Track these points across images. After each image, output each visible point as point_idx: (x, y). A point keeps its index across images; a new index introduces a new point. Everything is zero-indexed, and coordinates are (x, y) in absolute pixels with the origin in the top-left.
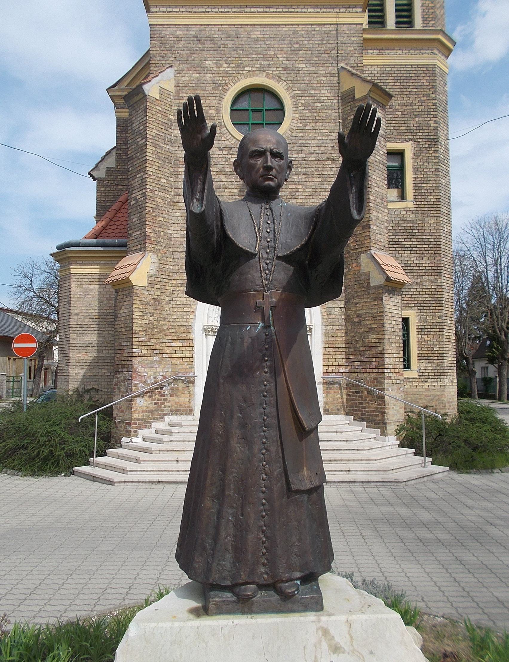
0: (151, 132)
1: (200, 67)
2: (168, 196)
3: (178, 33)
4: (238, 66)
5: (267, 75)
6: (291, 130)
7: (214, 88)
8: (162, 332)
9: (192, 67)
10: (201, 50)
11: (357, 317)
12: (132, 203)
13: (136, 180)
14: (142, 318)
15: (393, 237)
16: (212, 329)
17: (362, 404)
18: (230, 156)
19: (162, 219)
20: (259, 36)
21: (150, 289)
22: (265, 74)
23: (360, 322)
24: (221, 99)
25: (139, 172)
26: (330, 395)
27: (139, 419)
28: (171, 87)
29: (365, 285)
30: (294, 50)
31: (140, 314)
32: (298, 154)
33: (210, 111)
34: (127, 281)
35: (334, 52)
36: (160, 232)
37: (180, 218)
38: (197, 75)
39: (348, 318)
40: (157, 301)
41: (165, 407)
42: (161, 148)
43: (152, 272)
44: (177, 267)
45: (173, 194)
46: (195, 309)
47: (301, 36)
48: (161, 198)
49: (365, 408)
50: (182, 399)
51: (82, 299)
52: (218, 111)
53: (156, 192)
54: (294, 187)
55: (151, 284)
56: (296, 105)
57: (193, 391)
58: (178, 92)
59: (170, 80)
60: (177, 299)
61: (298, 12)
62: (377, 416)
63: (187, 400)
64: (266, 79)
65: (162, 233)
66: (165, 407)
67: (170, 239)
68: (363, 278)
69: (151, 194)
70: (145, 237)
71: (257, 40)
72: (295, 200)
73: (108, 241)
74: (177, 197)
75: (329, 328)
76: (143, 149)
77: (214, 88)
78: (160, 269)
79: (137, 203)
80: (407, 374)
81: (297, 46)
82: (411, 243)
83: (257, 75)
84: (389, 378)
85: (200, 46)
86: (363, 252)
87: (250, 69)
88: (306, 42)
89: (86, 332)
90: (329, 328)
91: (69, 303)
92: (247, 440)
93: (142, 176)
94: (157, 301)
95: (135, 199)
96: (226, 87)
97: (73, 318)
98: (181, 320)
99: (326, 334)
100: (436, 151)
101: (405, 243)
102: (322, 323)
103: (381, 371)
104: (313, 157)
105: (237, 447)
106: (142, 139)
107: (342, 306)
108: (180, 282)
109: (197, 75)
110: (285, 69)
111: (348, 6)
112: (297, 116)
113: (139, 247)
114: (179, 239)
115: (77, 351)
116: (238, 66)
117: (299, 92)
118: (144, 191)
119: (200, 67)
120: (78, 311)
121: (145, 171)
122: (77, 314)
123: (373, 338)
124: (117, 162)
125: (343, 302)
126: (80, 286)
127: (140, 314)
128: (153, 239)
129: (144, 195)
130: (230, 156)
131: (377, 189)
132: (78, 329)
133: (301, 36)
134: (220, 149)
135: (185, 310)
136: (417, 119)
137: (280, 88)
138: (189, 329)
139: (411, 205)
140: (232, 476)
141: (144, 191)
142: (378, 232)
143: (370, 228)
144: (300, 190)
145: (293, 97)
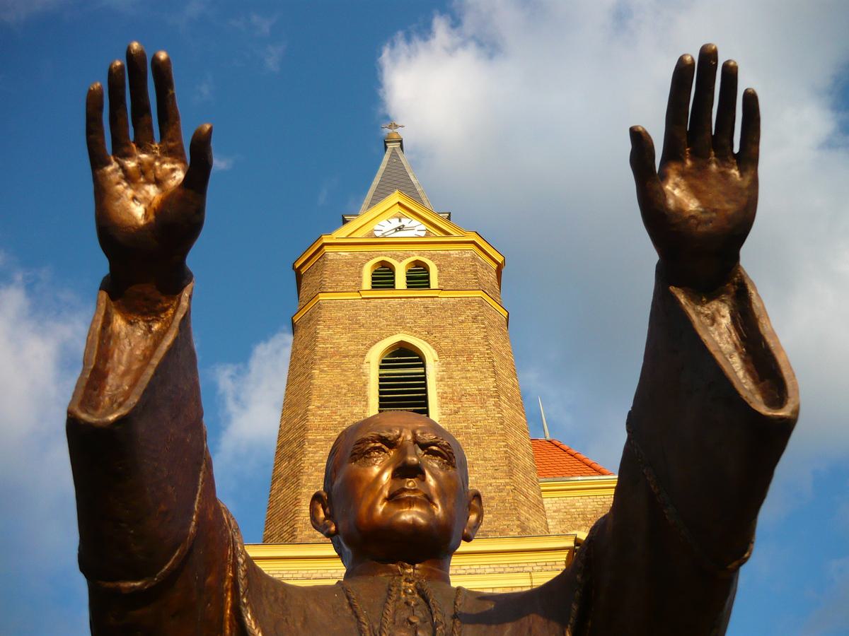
61: (470, 574)
111: (545, 564)
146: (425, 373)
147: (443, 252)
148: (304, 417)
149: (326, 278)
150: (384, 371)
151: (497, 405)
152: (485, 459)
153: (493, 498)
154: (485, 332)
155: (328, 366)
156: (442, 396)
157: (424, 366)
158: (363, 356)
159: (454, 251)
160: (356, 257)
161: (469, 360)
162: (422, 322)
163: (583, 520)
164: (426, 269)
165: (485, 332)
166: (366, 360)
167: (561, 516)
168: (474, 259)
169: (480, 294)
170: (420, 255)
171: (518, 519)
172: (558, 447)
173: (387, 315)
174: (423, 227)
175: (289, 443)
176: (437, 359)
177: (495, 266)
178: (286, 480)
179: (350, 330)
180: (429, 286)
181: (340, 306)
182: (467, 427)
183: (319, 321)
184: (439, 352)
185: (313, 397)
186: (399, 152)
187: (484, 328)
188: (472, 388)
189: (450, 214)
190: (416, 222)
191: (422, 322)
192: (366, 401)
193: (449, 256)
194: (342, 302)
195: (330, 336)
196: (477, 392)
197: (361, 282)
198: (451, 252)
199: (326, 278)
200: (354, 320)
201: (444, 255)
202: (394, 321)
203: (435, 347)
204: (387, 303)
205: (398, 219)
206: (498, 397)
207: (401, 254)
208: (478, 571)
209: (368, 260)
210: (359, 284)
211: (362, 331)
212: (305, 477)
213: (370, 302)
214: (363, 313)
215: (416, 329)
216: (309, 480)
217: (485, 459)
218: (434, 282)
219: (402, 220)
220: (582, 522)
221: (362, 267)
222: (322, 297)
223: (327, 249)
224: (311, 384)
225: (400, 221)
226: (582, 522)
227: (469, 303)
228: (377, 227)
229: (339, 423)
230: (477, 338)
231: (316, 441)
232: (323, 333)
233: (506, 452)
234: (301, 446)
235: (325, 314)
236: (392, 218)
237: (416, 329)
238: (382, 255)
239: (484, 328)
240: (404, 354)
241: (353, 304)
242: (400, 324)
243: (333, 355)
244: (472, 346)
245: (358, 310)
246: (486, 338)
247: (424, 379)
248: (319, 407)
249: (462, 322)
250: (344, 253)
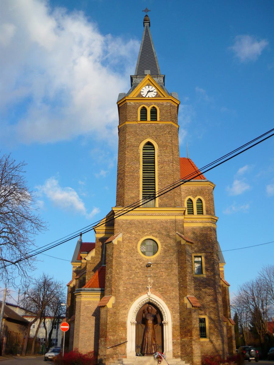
0: (115, 255)
1: (131, 233)
2: (119, 276)
3: (124, 222)
4: (143, 232)
5: (153, 236)
6: (161, 254)
7: (135, 240)
8: (117, 324)
9: (128, 232)
10: (131, 227)
11: (184, 318)
12: (107, 278)
13: (109, 271)
14: (110, 319)
15: (198, 287)
16: (133, 323)
17: (185, 350)
18: (140, 262)
19: (117, 284)
20: (150, 223)
21: (113, 309)
22: (152, 235)
23: (184, 320)
24: (137, 243)
25: (110, 268)
26: (175, 347)
27: (108, 354)
28: (121, 240)
29: (186, 307)
30: (161, 227)
31: (109, 317)
32: (163, 261)
33: (134, 247)
34: (106, 306)
35: (174, 228)
36: (116, 289)
37: (123, 283)
38: (129, 235)
39: (180, 319)
40: (115, 313)
41: (117, 351)
42: (117, 260)
43: (114, 303)
44: (121, 301)
45: (121, 275)
46: (128, 315)
47: (164, 223)
48: (117, 277)
49: (186, 351)
50: (122, 348)
51: (85, 310)
52: (136, 247)
53: (115, 275)
54: (162, 273)
55: (113, 307)
56: (162, 245)
57: (126, 345)
58: (123, 241)
59: (120, 237)
60: (121, 312)
62: (190, 354)
63: (124, 348)
64: (152, 237)
65: (117, 289)
66: (117, 351)
67: (119, 291)
68: (185, 305)
69: (114, 276)
70: (112, 291)
71: (149, 224)
72: (162, 278)
73: (95, 289)
74: (122, 276)
75: (174, 322)
76: (111, 261)
77: (135, 240)
78: (116, 302)
79: (109, 278)
80: (203, 340)
81: (162, 226)
82: (205, 290)
83: (149, 235)
84: (194, 340)
85: (130, 226)
86: (184, 296)
87: (147, 233)
88: (165, 225)
89: (86, 323)
90: (174, 322)
91: (80, 311)
92: (148, 339)
93: (111, 270)
94: (115, 313)
95: (108, 277)
96: (139, 239)
97: (81, 317)
98: (122, 319)
99: (173, 325)
100: (213, 256)
101: (203, 290)
102: (172, 321)
103: (191, 338)
104: (168, 263)
105: (147, 339)
106: (111, 257)
107: (178, 315)
108: (122, 306)
109: (129, 235)
110: (158, 233)
112: (162, 249)
113: (109, 294)
114: (122, 291)
115: (82, 330)
116: (143, 232)
117: (163, 241)
118: (111, 275)
119: (131, 233)
120: (83, 314)
121: (112, 269)
122: (83, 316)
123: (189, 327)
124: (95, 254)
125: (179, 313)
126: (84, 305)
127: (109, 317)
128: (114, 291)
129: (112, 276)
130: (140, 262)
131: (189, 274)
132: (83, 321)
133: (164, 223)
134: (137, 260)
135: (124, 316)
136: (206, 245)
137: (157, 240)
138: (125, 323)
139: (205, 276)
140: (146, 342)
141: (111, 275)
142: (190, 289)
143: (187, 287)
144: (164, 274)
145: (161, 243)
146: (154, 152)
147: (161, 103)
148: (124, 168)
149: (127, 114)
150: (144, 174)
151: (172, 165)
152: (168, 183)
153: (169, 195)
154: (171, 138)
155: (129, 150)
156: (159, 162)
157: (154, 149)
158: (138, 147)
159: (165, 102)
160: (136, 105)
161: (166, 149)
162: (155, 134)
163: (192, 193)
164: (156, 109)
165: (171, 138)
166: (139, 149)
167: (186, 191)
168: (171, 106)
169: (171, 123)
170: (154, 104)
171: (174, 201)
172: (190, 162)
173: (145, 130)
174: (156, 91)
175: (121, 174)
176: (158, 148)
177: (177, 105)
178: (120, 186)
179: (135, 137)
180: (157, 120)
181: (131, 126)
182: (164, 173)
183: (126, 132)
184: (159, 146)
185: (126, 161)
186: (148, 27)
187: (171, 137)
188: (166, 159)
189: (165, 75)
190: (154, 88)
191: (155, 134)
192: (139, 163)
193: (163, 104)
194: (132, 125)
195: (130, 139)
196: (168, 161)
197: (137, 116)
198: (164, 103)
199: (127, 114)
200: (135, 132)
201: (162, 104)
202: (147, 133)
203: (157, 144)
204: (145, 125)
205: (148, 86)
206: (173, 163)
207: (149, 103)
208: (164, 215)
209: (139, 106)
210: (137, 117)
211: (138, 137)
212: (125, 187)
213: (140, 125)
214: (138, 129)
215: (153, 136)
216: (127, 188)
217: (168, 183)
218: (158, 119)
219: (150, 86)
220: (191, 194)
221: (137, 109)
222: (127, 123)
223: (127, 101)
224: (126, 157)
225: (149, 87)
226: (191, 194)
227: (168, 126)
228: (142, 91)
229: (133, 170)
230: (169, 141)
231: (127, 176)
232: (128, 138)
233: (173, 181)
234: (124, 176)
235: (128, 130)
236: (146, 86)
237: (153, 136)
238: (143, 104)
239: (171, 137)
240: (149, 143)
241: (135, 125)
242: (149, 135)
243: (131, 146)
244: (167, 144)
245: (137, 128)
246: (171, 141)
247: (154, 154)
248: (128, 165)
249: (165, 134)
250: (132, 103)
